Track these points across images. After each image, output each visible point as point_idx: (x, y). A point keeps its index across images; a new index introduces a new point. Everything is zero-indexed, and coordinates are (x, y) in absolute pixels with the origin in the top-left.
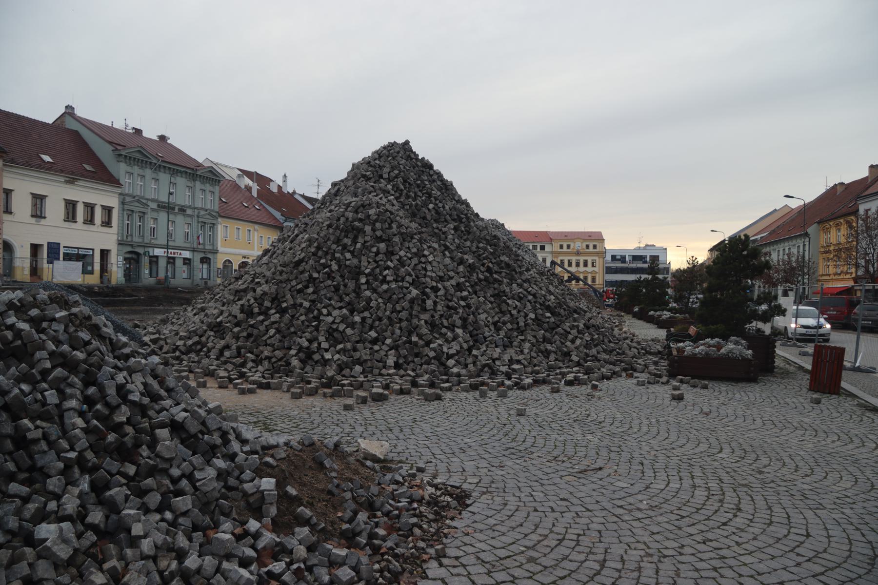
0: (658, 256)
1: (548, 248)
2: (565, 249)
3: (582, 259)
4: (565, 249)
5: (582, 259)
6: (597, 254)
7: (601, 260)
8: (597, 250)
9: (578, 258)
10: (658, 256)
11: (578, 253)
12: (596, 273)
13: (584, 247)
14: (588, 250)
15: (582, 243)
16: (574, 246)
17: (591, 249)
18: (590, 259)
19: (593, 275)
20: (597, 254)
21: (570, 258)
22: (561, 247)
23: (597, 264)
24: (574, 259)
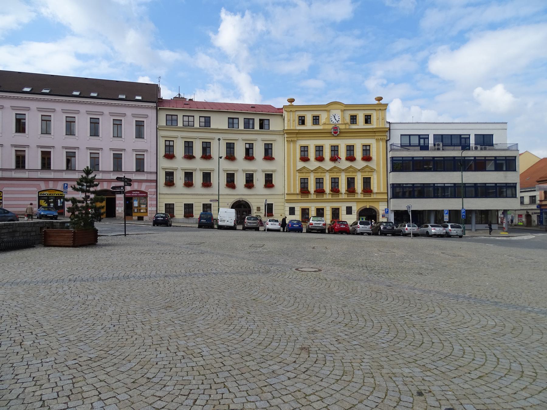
0: (492, 135)
1: (275, 124)
2: (309, 125)
3: (342, 144)
4: (309, 125)
5: (342, 144)
6: (373, 133)
7: (382, 144)
8: (375, 124)
9: (335, 142)
10: (492, 135)
11: (336, 132)
12: (372, 170)
13: (348, 120)
14: (354, 127)
15: (343, 111)
16: (329, 118)
17: (361, 123)
18: (358, 144)
19: (367, 175)
20: (373, 133)
21: (319, 142)
22: (302, 121)
23: (373, 154)
24: (327, 144)
